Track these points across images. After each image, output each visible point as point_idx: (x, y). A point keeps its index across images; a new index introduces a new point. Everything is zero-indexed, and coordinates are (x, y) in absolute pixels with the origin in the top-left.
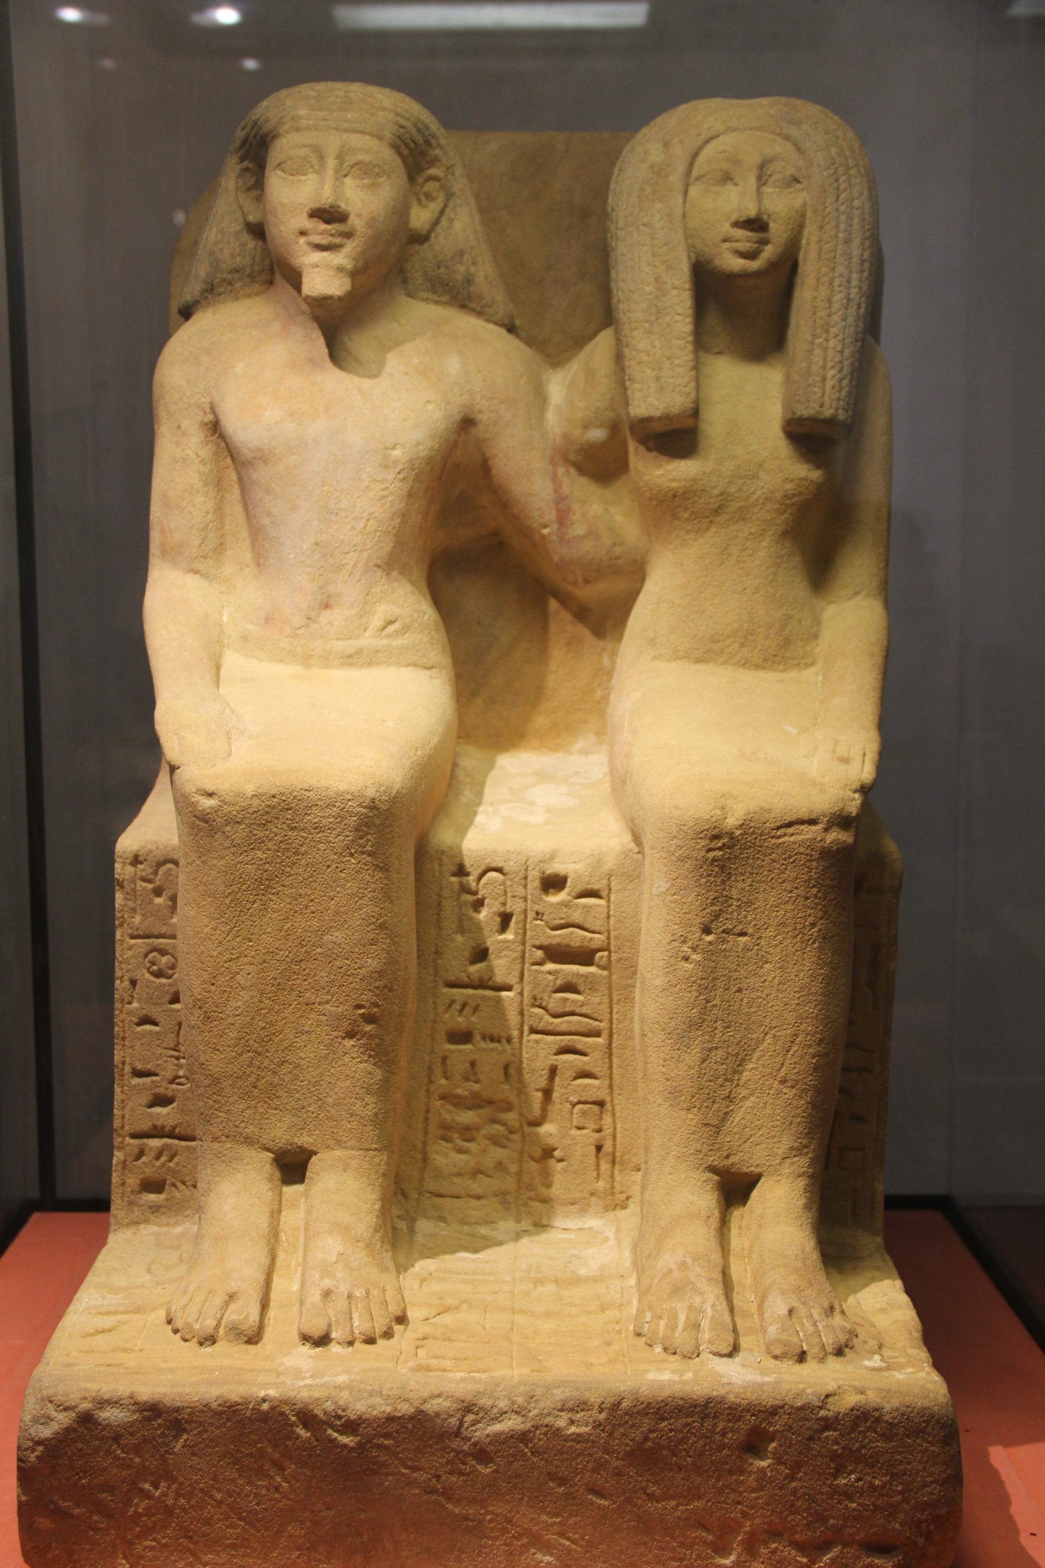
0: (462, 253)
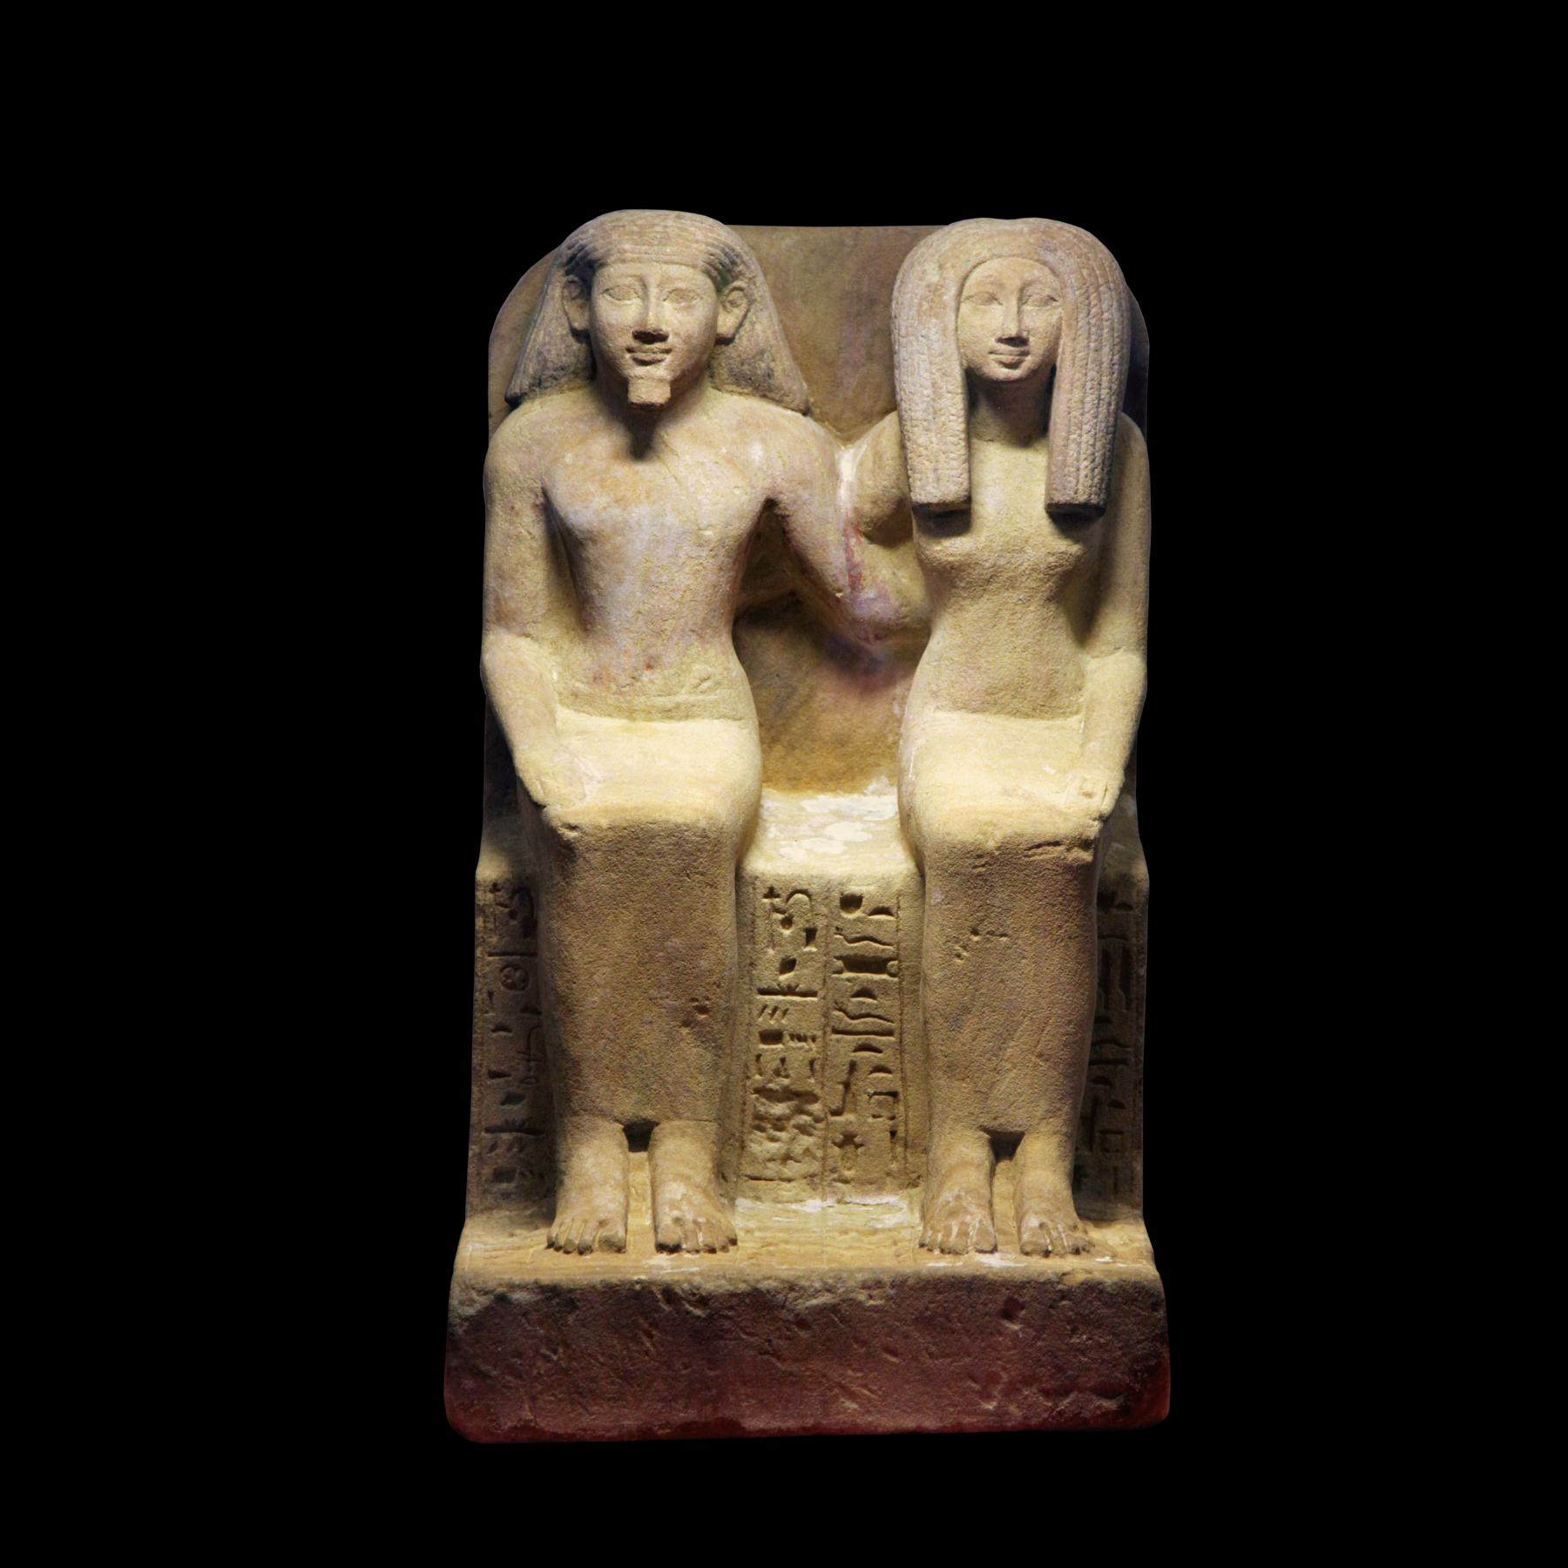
0: (762, 352)
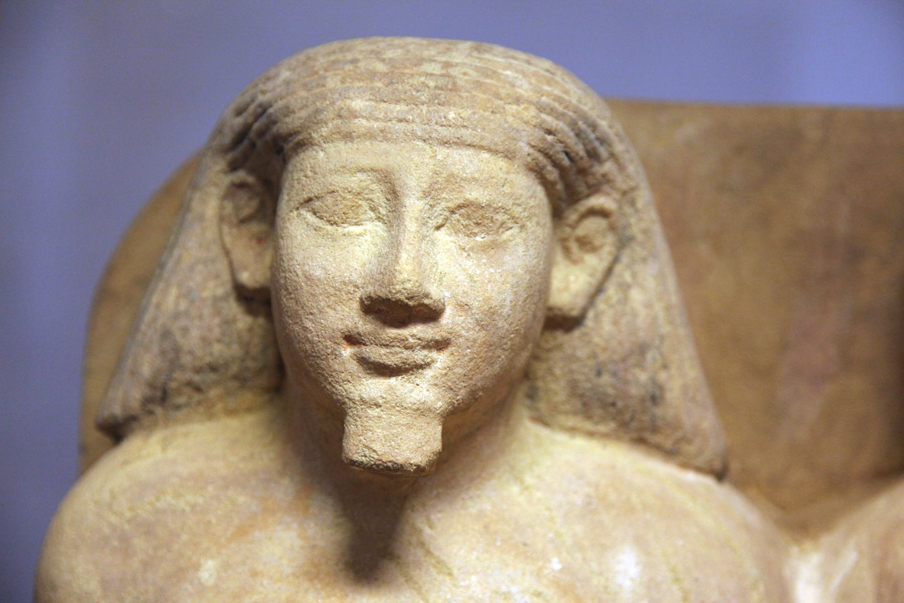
0: (642, 349)
